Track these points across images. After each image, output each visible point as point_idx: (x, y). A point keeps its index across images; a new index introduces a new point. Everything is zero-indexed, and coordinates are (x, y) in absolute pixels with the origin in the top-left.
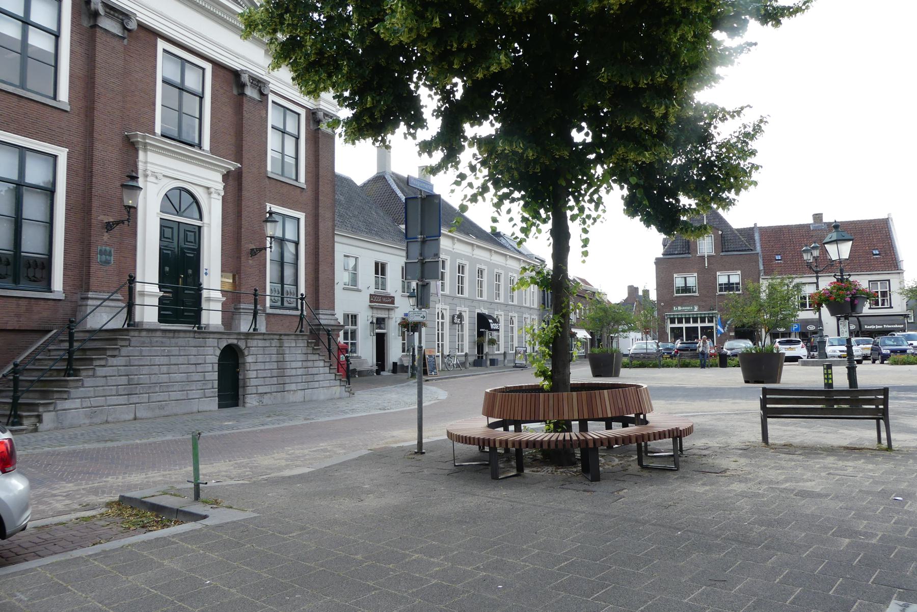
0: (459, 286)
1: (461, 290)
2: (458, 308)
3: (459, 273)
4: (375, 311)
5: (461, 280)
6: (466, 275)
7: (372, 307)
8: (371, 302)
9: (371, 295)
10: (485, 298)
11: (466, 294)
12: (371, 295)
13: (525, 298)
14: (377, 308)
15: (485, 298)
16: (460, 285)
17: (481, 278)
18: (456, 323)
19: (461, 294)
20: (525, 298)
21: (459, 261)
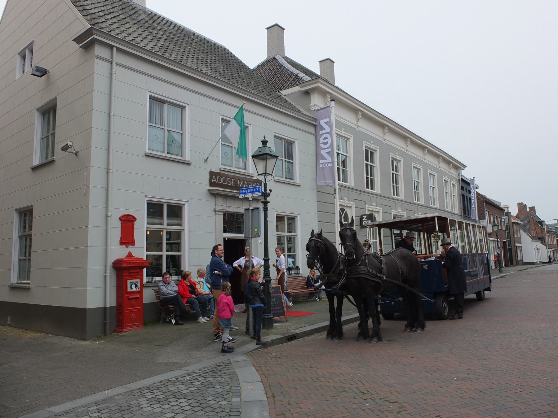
0: (367, 178)
1: (370, 183)
2: (368, 207)
3: (367, 160)
4: (220, 201)
5: (370, 170)
6: (377, 163)
7: (214, 195)
8: (211, 184)
9: (212, 174)
10: (402, 196)
11: (378, 189)
12: (212, 174)
13: (447, 201)
14: (226, 197)
15: (402, 196)
16: (369, 176)
17: (396, 172)
18: (366, 227)
19: (372, 189)
20: (447, 201)
21: (365, 144)
